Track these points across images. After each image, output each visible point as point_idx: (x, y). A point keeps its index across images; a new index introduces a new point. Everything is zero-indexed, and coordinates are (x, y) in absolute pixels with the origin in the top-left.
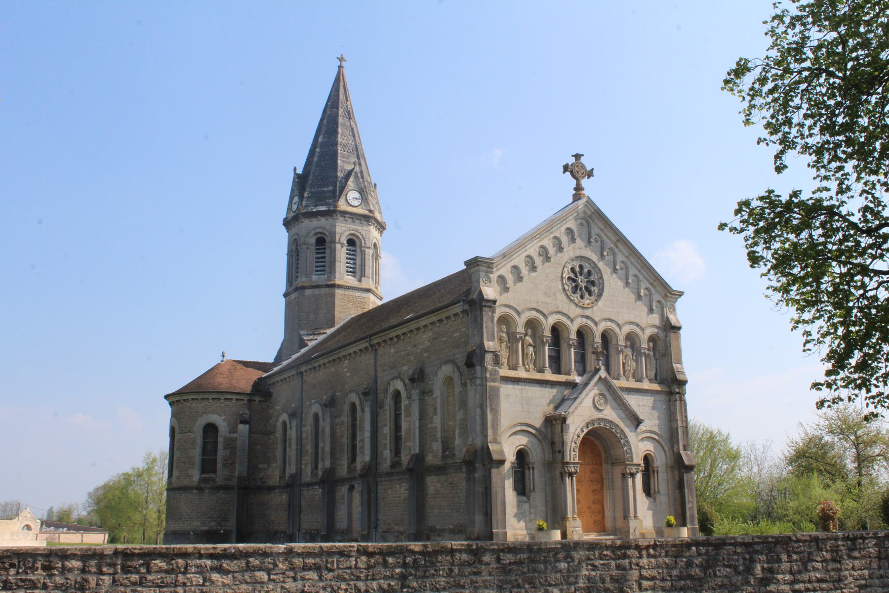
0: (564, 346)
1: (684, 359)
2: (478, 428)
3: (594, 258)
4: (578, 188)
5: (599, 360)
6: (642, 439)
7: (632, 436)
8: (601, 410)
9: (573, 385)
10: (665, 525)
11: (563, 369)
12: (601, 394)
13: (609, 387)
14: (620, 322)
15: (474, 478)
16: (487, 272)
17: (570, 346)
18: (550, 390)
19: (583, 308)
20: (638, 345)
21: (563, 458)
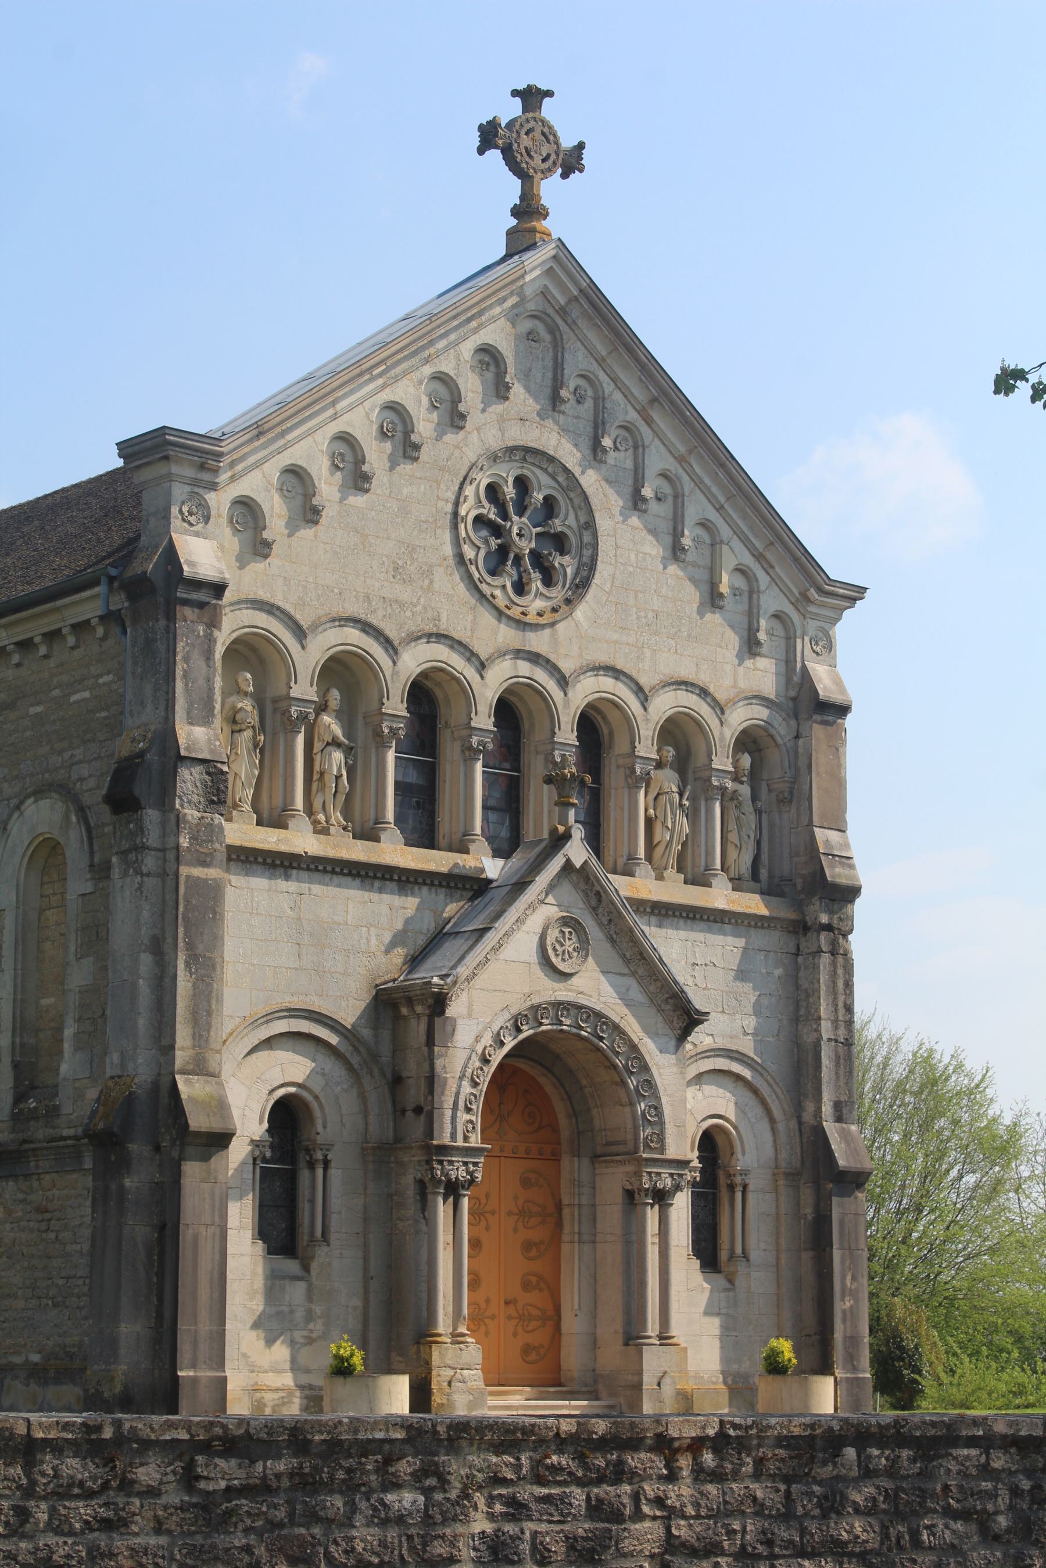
0: (450, 752)
1: (851, 816)
2: (142, 1023)
3: (570, 454)
4: (528, 209)
5: (564, 804)
6: (699, 1079)
7: (664, 1068)
8: (566, 976)
9: (476, 887)
10: (761, 1367)
11: (446, 824)
12: (568, 922)
13: (596, 897)
14: (644, 681)
15: (122, 1190)
16: (195, 483)
17: (470, 753)
18: (397, 900)
19: (522, 625)
20: (700, 760)
21: (430, 1134)
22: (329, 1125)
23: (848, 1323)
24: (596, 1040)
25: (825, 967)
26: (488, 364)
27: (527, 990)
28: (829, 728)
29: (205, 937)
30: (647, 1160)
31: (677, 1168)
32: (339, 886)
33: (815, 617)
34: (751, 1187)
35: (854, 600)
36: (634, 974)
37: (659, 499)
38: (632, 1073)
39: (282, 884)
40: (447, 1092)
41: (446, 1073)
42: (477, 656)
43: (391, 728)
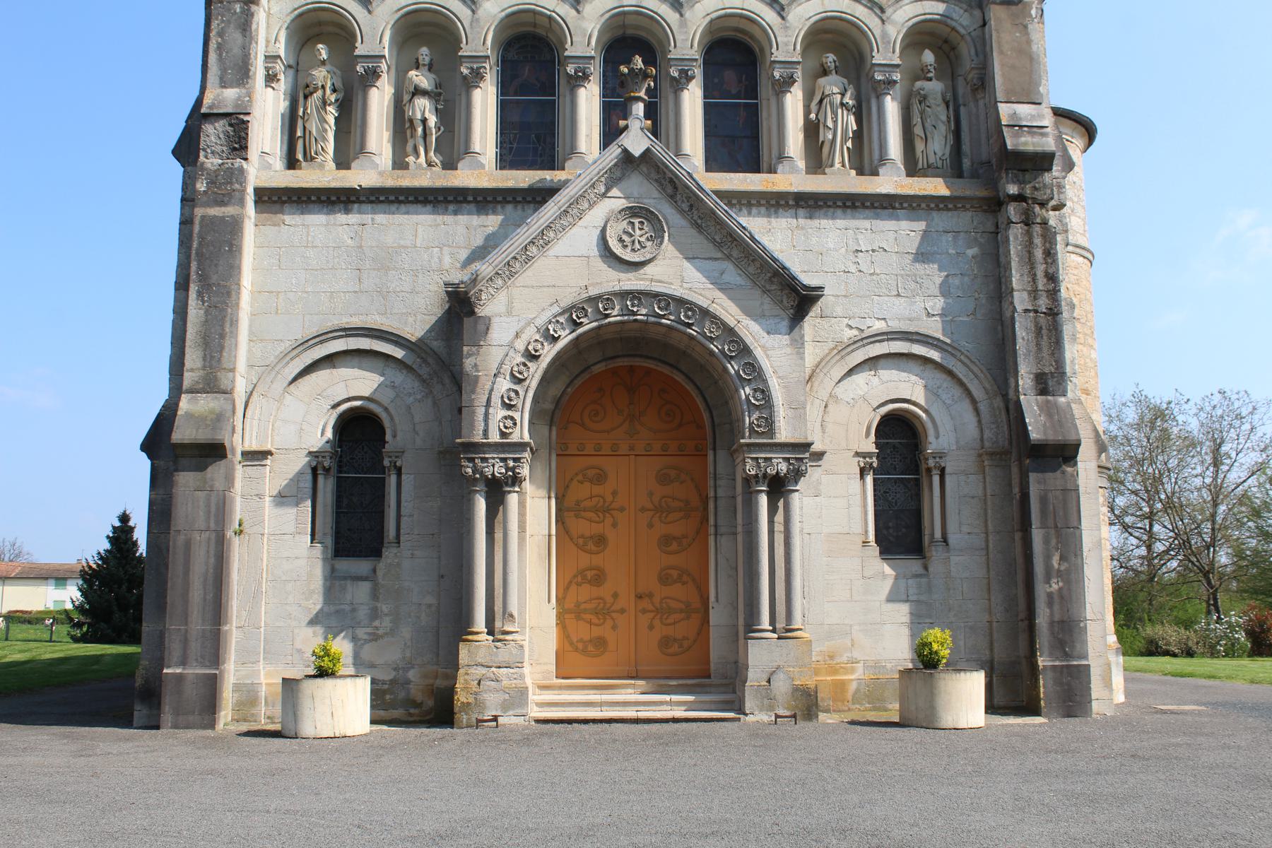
7: (770, 348)
12: (631, 212)
18: (475, 220)
22: (400, 435)
23: (1056, 607)
25: (1016, 238)
27: (583, 284)
28: (1013, 7)
29: (220, 268)
30: (748, 445)
31: (793, 452)
32: (407, 213)
34: (948, 470)
36: (728, 257)
38: (731, 357)
39: (341, 218)
40: (478, 390)
41: (478, 371)
43: (472, 69)
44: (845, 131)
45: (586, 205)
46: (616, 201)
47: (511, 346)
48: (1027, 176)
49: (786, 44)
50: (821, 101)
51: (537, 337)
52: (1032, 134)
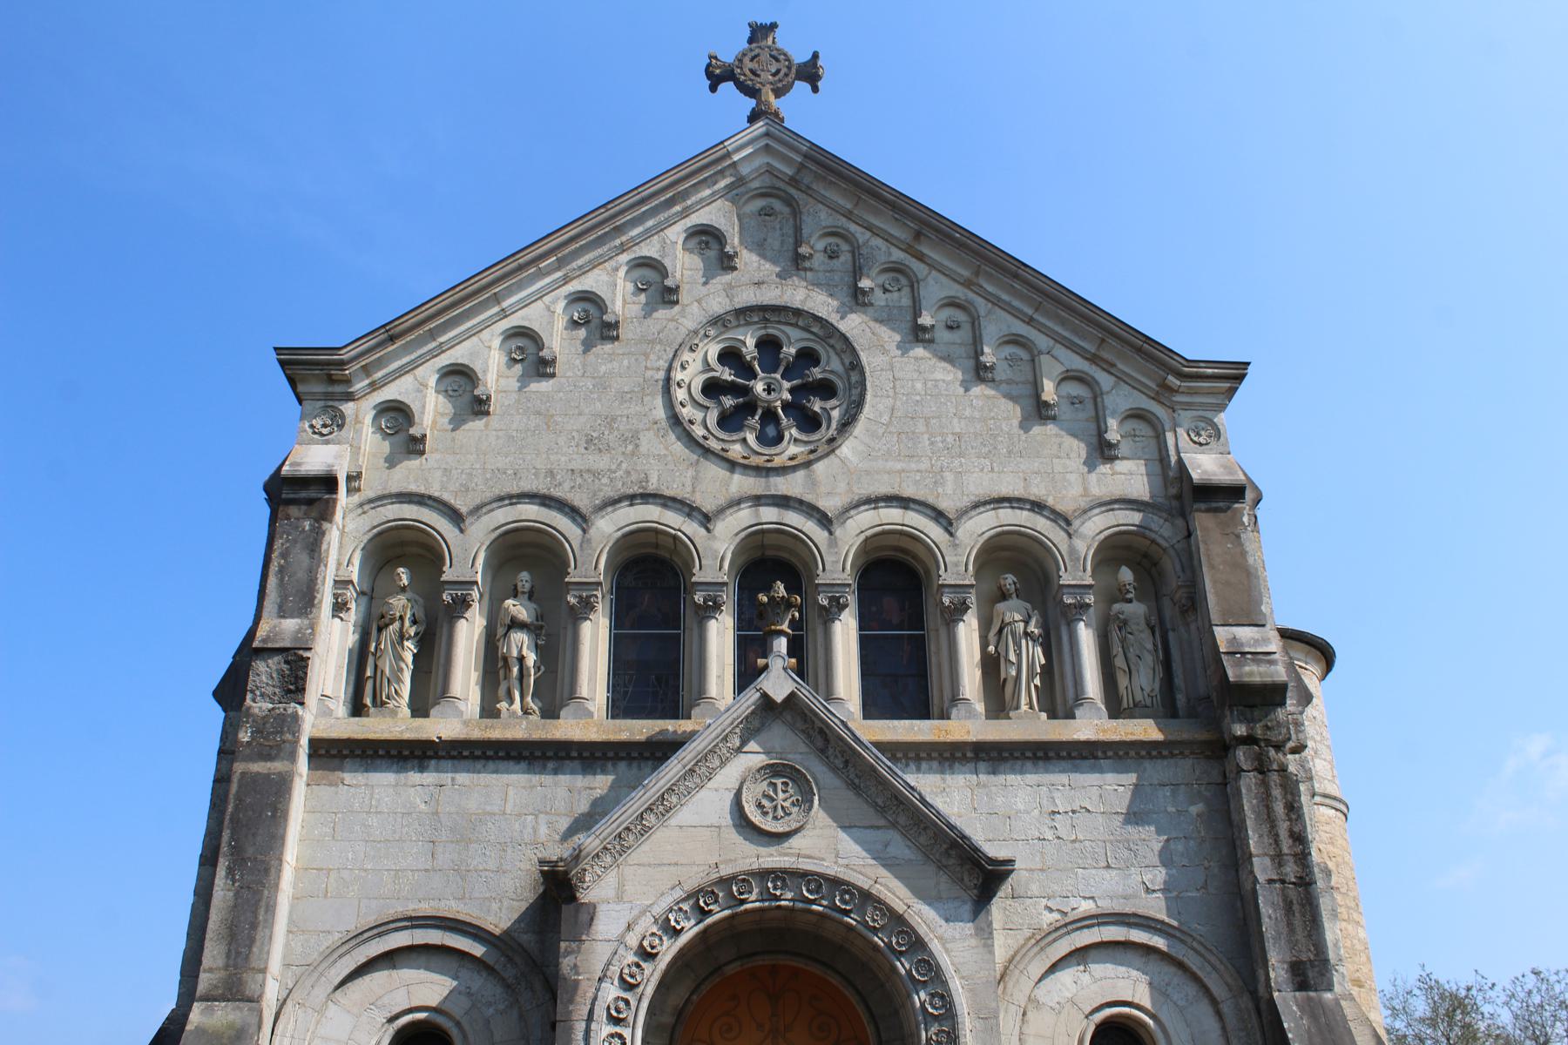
3: (822, 304)
7: (949, 941)
12: (773, 771)
14: (943, 505)
16: (328, 396)
18: (580, 781)
24: (838, 916)
25: (1249, 790)
26: (707, 243)
28: (1222, 515)
29: (259, 838)
32: (496, 772)
33: (1188, 406)
35: (1240, 378)
36: (894, 825)
37: (950, 328)
38: (901, 953)
39: (415, 777)
40: (578, 999)
41: (578, 974)
42: (698, 509)
44: (1031, 666)
45: (717, 762)
46: (754, 757)
47: (621, 941)
48: (1256, 713)
49: (956, 565)
50: (1000, 631)
51: (655, 929)
52: (1258, 662)
